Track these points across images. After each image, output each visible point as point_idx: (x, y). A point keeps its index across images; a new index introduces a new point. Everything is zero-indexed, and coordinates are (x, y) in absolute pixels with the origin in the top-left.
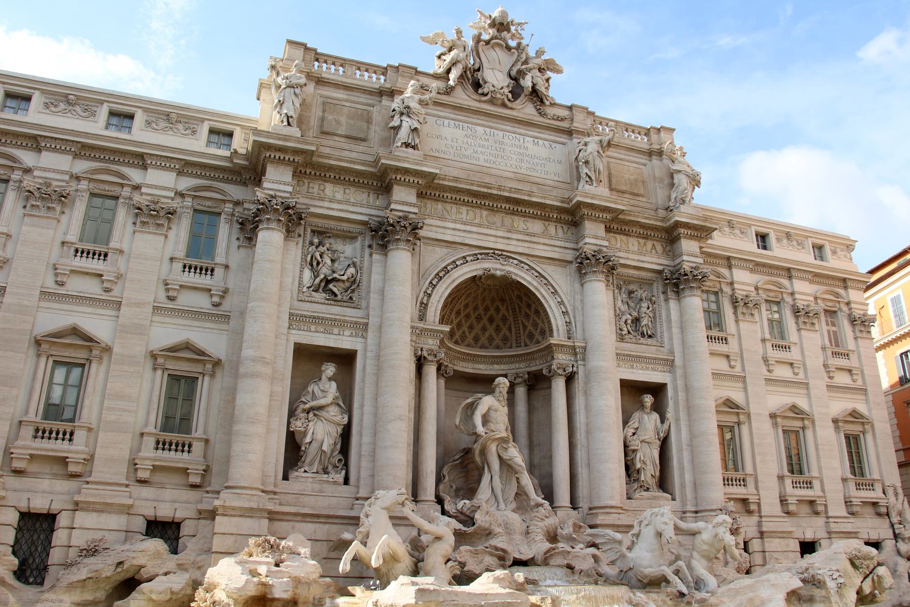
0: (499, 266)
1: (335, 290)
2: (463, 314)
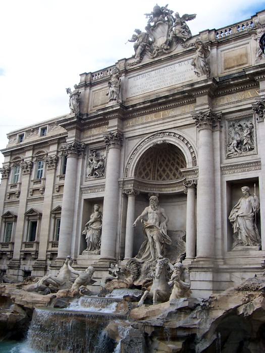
0: (160, 139)
1: (97, 173)
2: (164, 166)
